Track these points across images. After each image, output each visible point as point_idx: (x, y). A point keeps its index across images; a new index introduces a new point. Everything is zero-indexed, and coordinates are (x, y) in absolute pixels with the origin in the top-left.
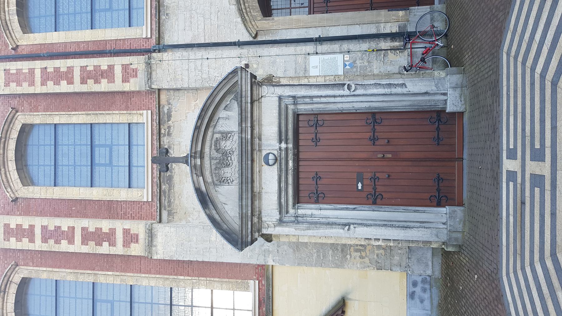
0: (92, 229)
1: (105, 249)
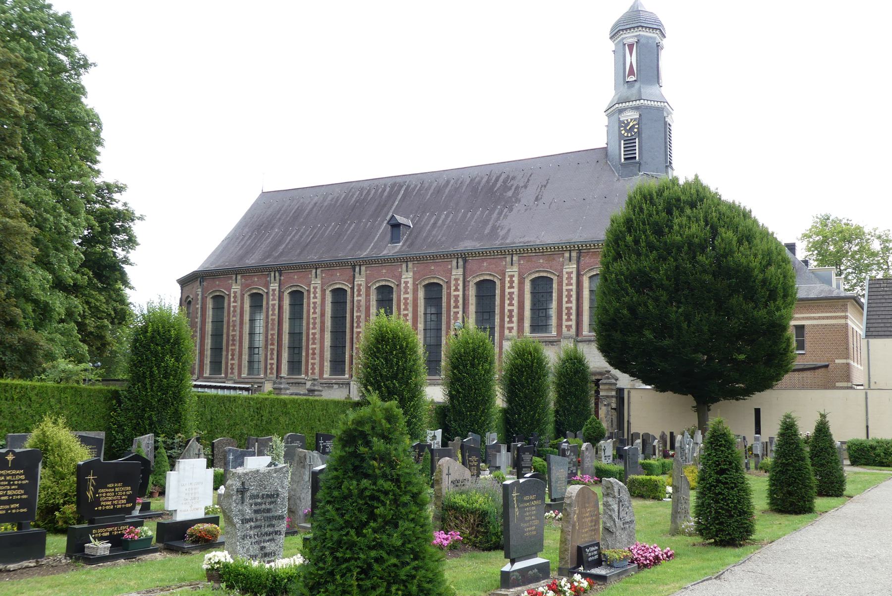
0: (513, 313)
1: (507, 319)
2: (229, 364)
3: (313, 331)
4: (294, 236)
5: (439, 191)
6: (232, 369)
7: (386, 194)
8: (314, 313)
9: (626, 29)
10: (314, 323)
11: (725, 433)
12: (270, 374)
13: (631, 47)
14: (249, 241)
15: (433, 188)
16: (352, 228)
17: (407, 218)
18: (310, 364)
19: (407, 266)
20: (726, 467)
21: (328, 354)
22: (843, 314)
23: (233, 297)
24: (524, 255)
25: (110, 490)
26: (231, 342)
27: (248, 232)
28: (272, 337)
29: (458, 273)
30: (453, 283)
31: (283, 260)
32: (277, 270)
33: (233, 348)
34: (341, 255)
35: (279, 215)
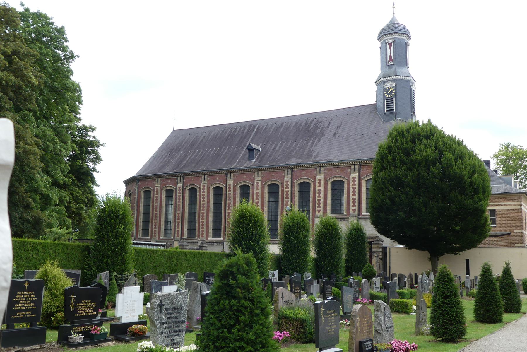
0: (321, 202)
1: (317, 205)
2: (153, 231)
3: (203, 212)
4: (192, 156)
5: (277, 129)
6: (155, 233)
7: (246, 131)
8: (203, 201)
9: (387, 34)
10: (203, 207)
11: (448, 274)
12: (177, 237)
13: (390, 44)
14: (166, 159)
15: (273, 128)
16: (225, 151)
17: (258, 145)
18: (200, 231)
19: (258, 174)
20: (448, 294)
21: (211, 225)
22: (519, 203)
23: (156, 191)
24: (327, 167)
25: (83, 304)
26: (154, 218)
27: (165, 154)
28: (179, 215)
29: (288, 178)
30: (285, 183)
31: (185, 170)
32: (182, 176)
33: (156, 221)
34: (219, 167)
35: (183, 144)
